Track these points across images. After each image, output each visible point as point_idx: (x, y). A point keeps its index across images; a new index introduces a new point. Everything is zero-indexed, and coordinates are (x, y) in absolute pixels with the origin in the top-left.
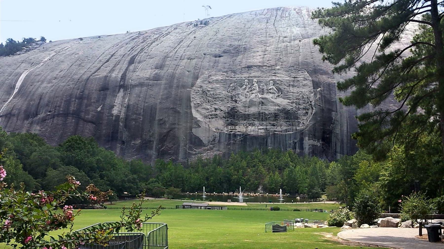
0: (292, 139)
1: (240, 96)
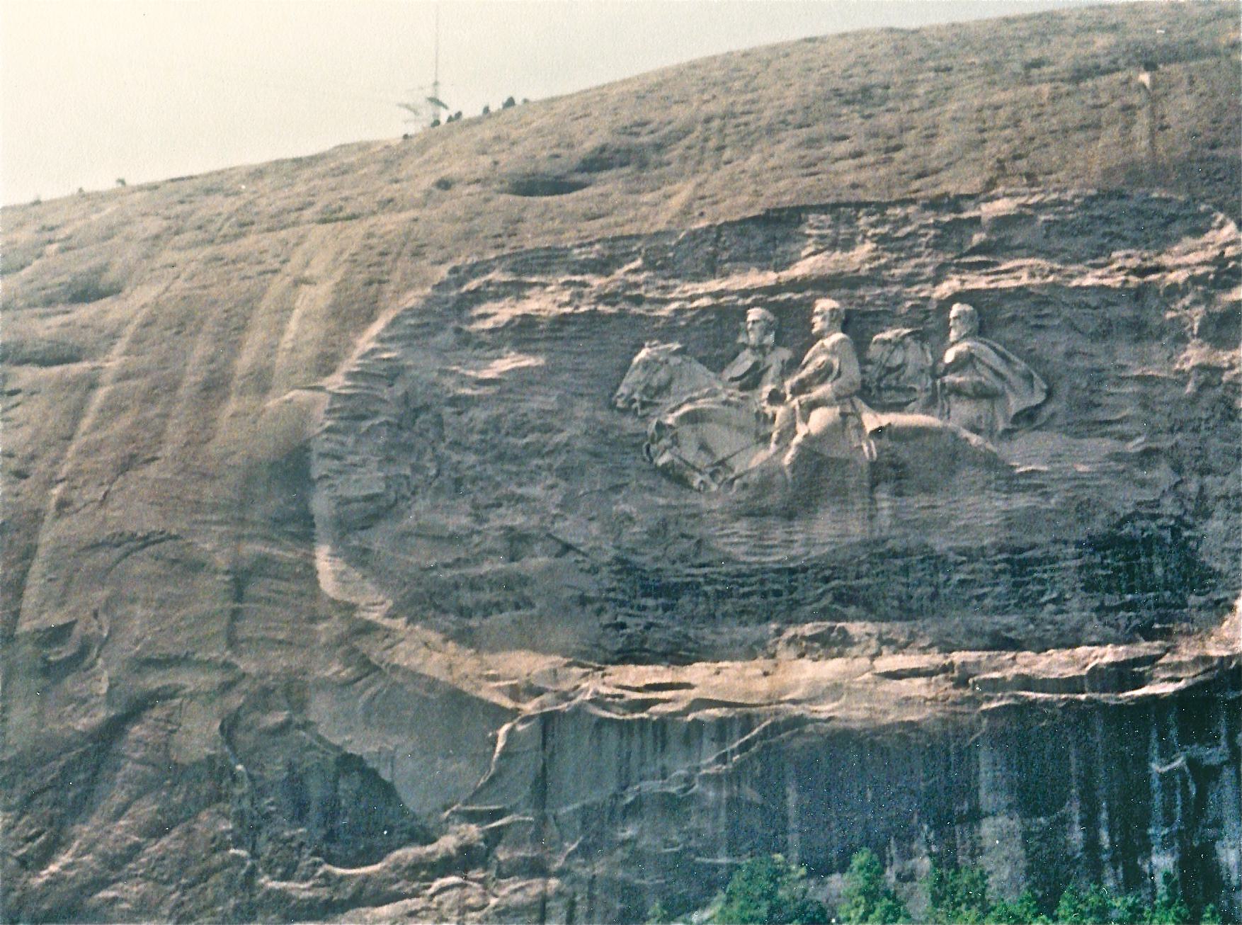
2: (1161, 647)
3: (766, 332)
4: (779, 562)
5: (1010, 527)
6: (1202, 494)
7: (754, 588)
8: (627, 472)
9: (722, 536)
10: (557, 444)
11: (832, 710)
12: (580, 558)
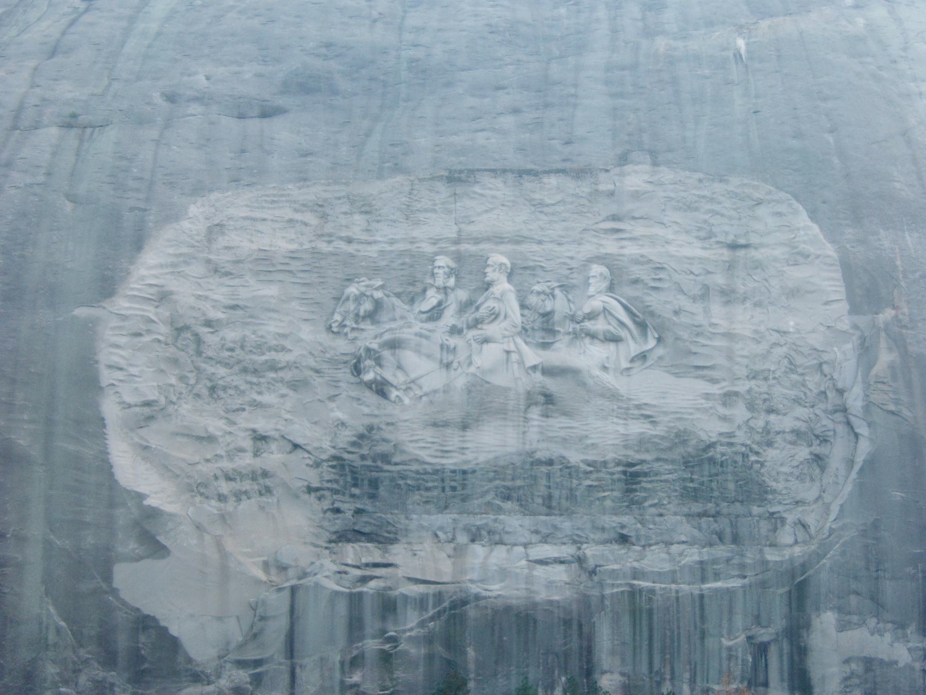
0: (739, 621)
1: (408, 357)
2: (732, 551)
3: (449, 275)
4: (455, 464)
5: (626, 447)
6: (766, 431)
7: (436, 484)
8: (341, 384)
9: (411, 441)
10: (288, 362)
11: (499, 590)
12: (307, 455)
